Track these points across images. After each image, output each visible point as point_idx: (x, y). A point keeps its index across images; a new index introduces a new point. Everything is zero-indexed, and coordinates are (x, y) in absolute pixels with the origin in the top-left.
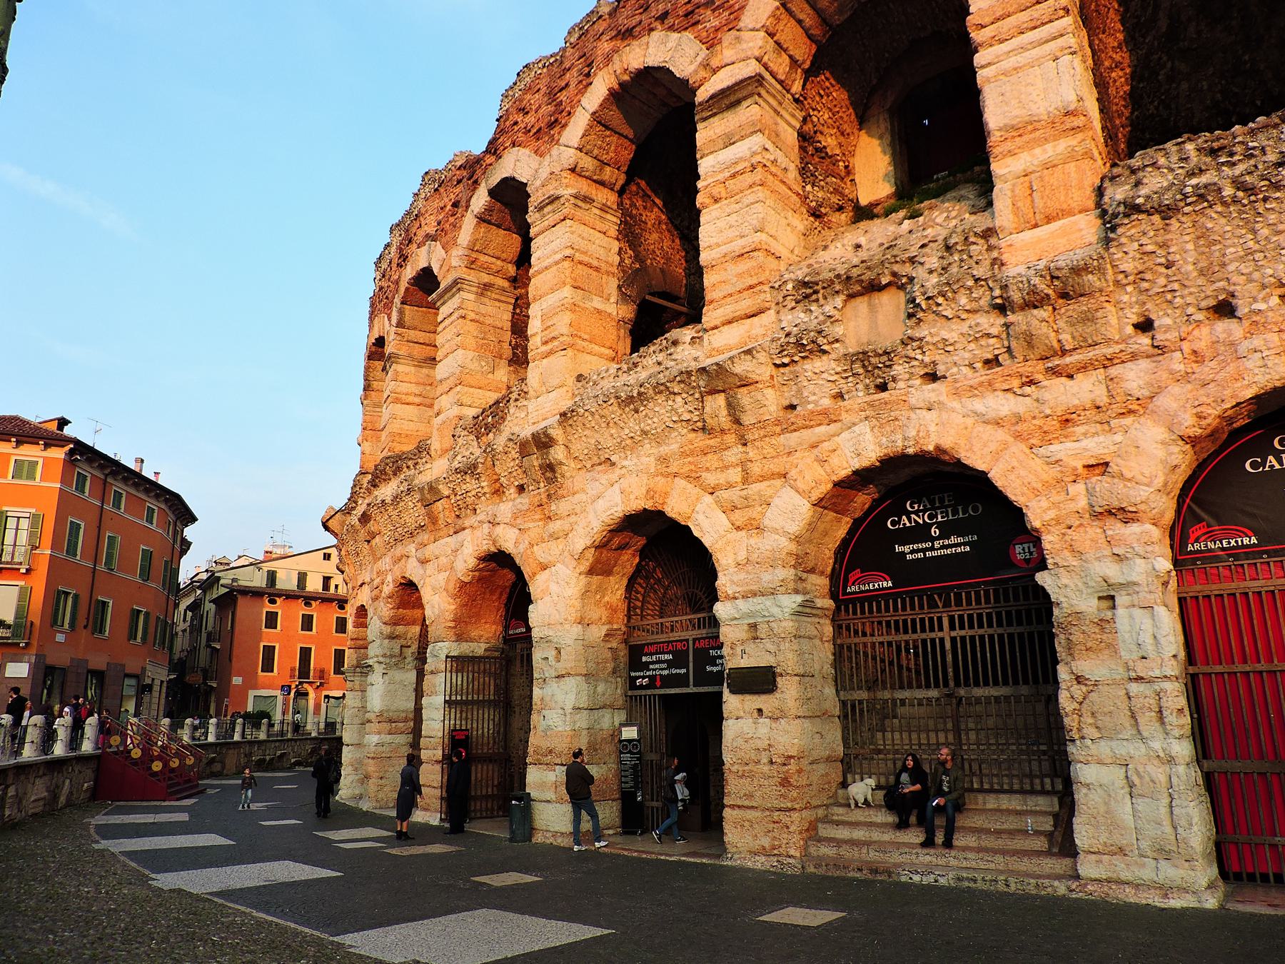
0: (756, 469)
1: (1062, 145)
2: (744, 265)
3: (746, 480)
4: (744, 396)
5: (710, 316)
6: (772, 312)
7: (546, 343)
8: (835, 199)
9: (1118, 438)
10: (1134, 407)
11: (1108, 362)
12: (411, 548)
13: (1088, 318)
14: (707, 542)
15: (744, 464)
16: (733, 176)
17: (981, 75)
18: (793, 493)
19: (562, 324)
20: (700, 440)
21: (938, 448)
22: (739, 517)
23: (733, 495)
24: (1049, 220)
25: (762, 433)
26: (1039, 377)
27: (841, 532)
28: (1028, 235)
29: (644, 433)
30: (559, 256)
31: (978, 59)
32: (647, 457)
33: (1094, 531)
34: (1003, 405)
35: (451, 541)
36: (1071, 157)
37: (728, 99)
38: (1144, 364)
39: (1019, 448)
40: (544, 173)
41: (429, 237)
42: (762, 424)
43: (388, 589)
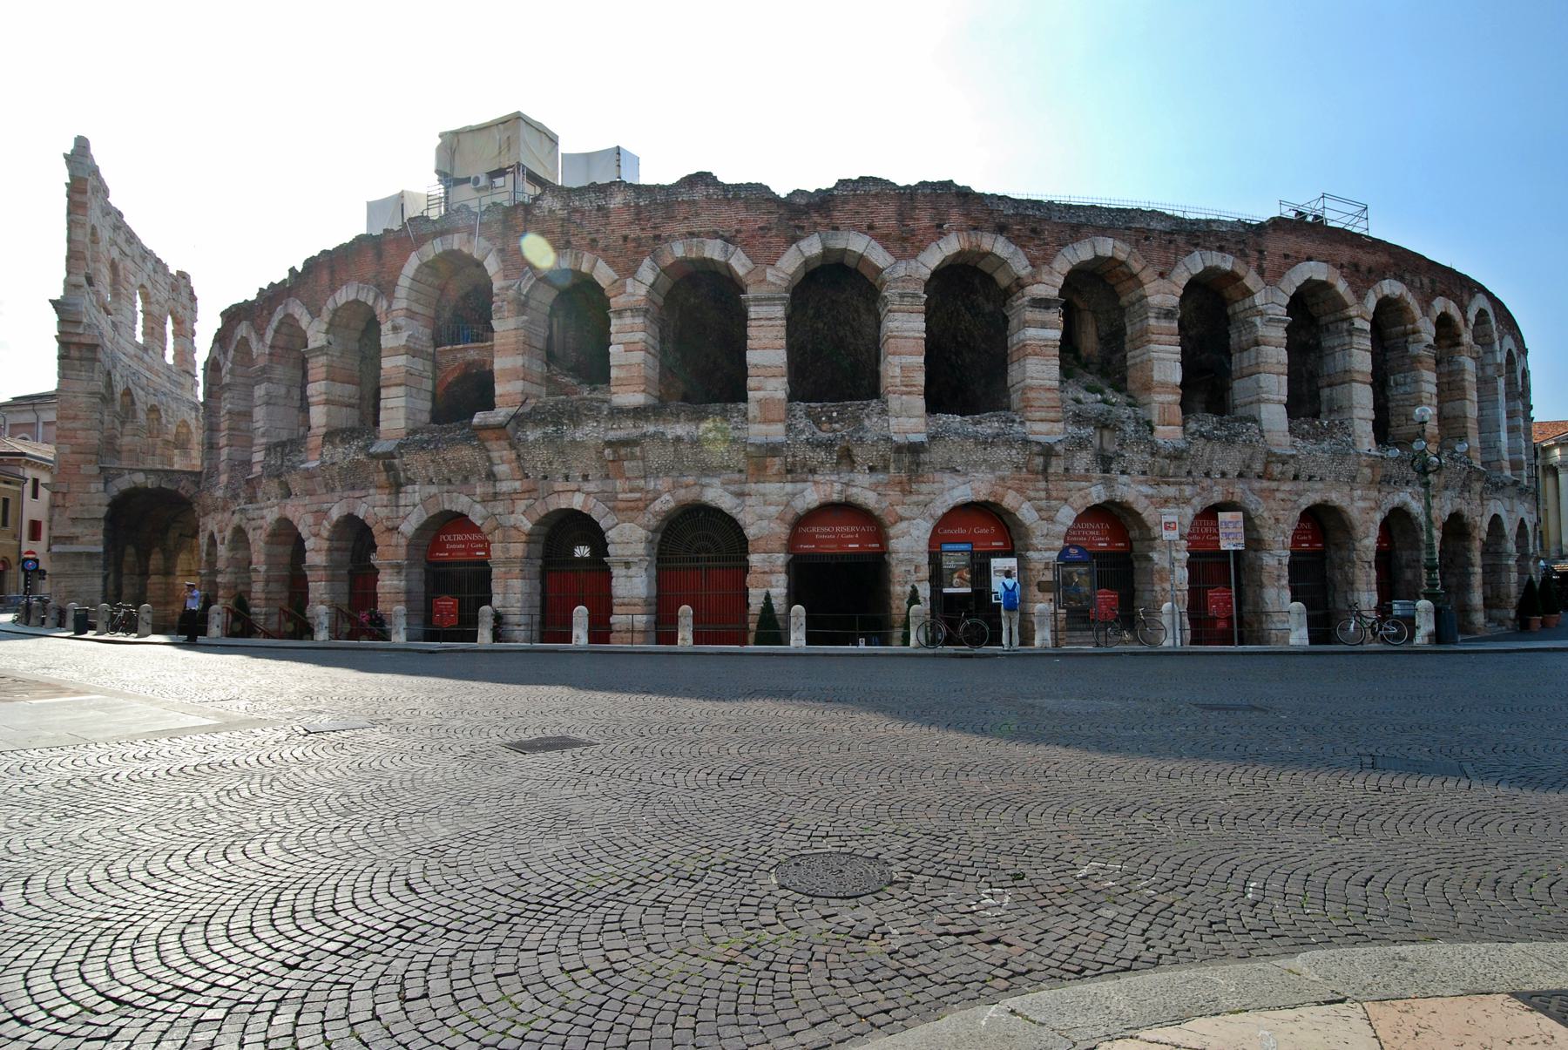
0: (1054, 494)
2: (1049, 395)
3: (1048, 498)
10: (1187, 501)
12: (716, 481)
13: (1179, 467)
14: (1027, 523)
15: (1047, 490)
22: (1044, 514)
23: (1043, 503)
34: (1150, 491)
35: (789, 487)
37: (1042, 303)
40: (901, 270)
41: (716, 235)
42: (1056, 474)
43: (657, 506)
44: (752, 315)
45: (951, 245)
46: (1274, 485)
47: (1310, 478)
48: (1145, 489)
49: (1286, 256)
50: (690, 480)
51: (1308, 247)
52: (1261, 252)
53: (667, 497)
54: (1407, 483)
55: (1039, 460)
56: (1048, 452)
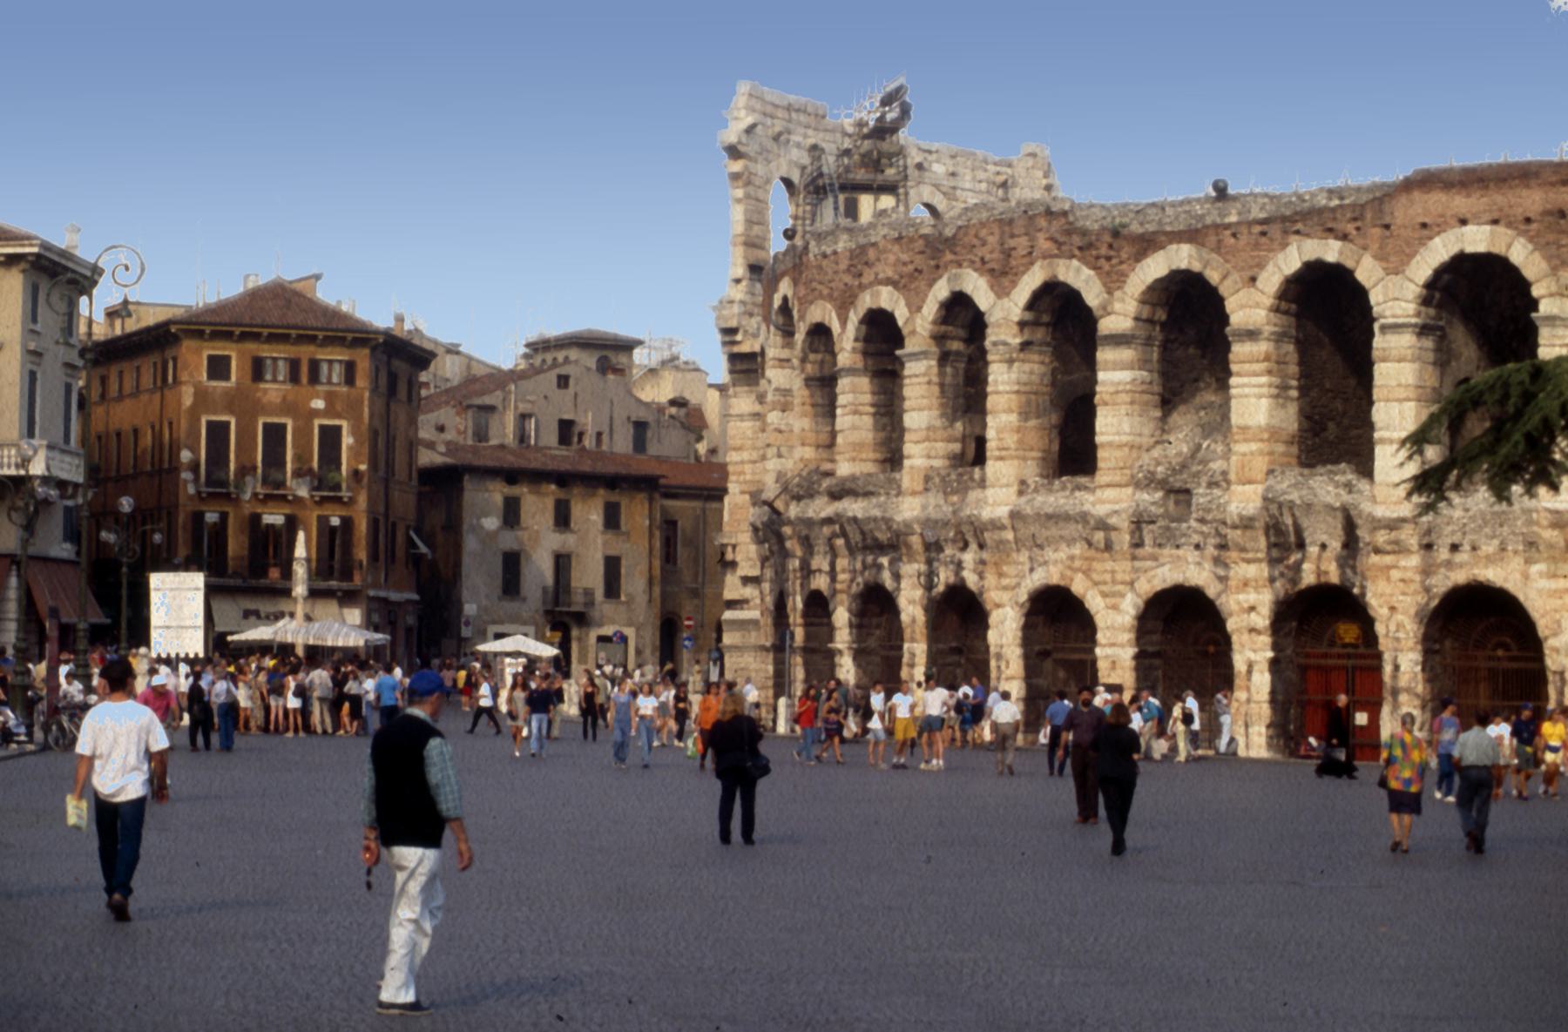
0: (1119, 577)
2: (1118, 454)
4: (1113, 535)
5: (1101, 477)
7: (999, 449)
17: (1233, 391)
19: (1011, 440)
20: (1092, 553)
23: (1104, 588)
24: (1250, 482)
28: (1240, 488)
29: (1061, 537)
30: (1008, 388)
31: (1233, 381)
32: (1063, 553)
36: (1261, 453)
37: (1118, 340)
41: (888, 282)
44: (906, 372)
45: (1032, 280)
46: (1388, 559)
47: (1455, 548)
49: (1424, 225)
50: (870, 559)
51: (1460, 203)
52: (1387, 227)
53: (860, 580)
55: (1099, 536)
56: (1102, 525)
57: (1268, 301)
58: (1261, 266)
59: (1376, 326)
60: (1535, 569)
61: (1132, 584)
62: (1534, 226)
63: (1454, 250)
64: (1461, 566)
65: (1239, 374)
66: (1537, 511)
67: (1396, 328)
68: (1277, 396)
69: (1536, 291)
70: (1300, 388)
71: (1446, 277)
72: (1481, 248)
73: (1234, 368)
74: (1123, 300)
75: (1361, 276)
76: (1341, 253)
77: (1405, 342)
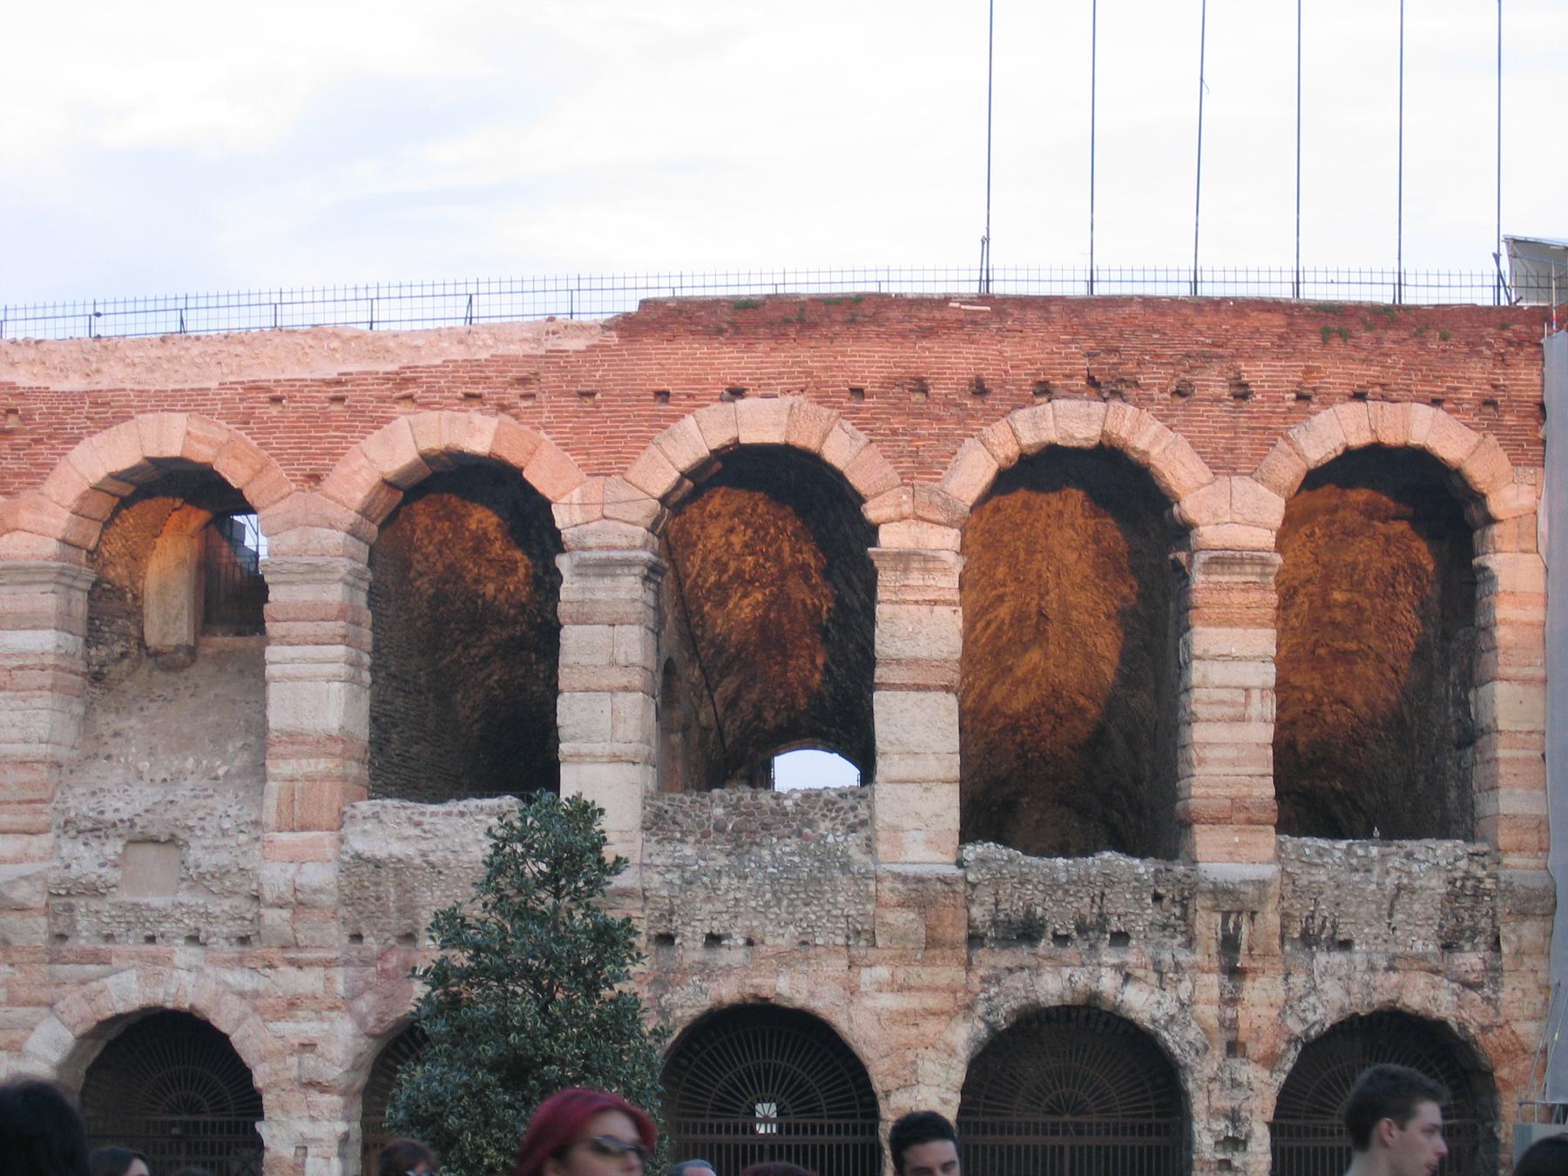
1: (322, 765)
2: (24, 776)
6: (51, 835)
8: (118, 649)
9: (326, 1026)
11: (327, 964)
16: (21, 668)
17: (271, 670)
18: (57, 1022)
21: (192, 1006)
24: (303, 828)
25: (32, 958)
26: (276, 962)
27: (96, 1053)
28: (286, 837)
31: (272, 652)
33: (298, 1096)
36: (327, 777)
38: (351, 971)
39: (255, 1020)
47: (713, 940)
48: (241, 979)
49: (663, 396)
54: (1121, 938)
57: (351, 517)
58: (334, 455)
59: (563, 562)
60: (866, 976)
61: (51, 1005)
62: (869, 402)
63: (719, 439)
64: (728, 971)
65: (286, 641)
66: (878, 880)
67: (606, 568)
68: (351, 680)
69: (872, 512)
70: (373, 670)
71: (688, 483)
72: (773, 436)
73: (272, 628)
74: (38, 508)
75: (537, 476)
76: (497, 438)
77: (629, 590)
